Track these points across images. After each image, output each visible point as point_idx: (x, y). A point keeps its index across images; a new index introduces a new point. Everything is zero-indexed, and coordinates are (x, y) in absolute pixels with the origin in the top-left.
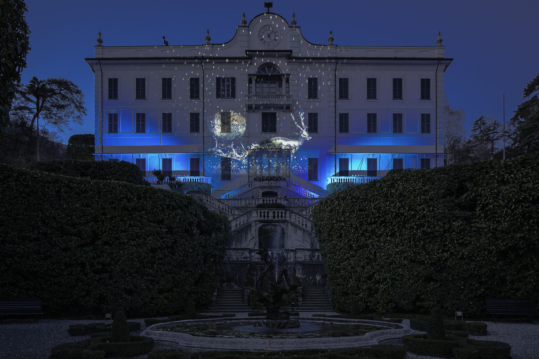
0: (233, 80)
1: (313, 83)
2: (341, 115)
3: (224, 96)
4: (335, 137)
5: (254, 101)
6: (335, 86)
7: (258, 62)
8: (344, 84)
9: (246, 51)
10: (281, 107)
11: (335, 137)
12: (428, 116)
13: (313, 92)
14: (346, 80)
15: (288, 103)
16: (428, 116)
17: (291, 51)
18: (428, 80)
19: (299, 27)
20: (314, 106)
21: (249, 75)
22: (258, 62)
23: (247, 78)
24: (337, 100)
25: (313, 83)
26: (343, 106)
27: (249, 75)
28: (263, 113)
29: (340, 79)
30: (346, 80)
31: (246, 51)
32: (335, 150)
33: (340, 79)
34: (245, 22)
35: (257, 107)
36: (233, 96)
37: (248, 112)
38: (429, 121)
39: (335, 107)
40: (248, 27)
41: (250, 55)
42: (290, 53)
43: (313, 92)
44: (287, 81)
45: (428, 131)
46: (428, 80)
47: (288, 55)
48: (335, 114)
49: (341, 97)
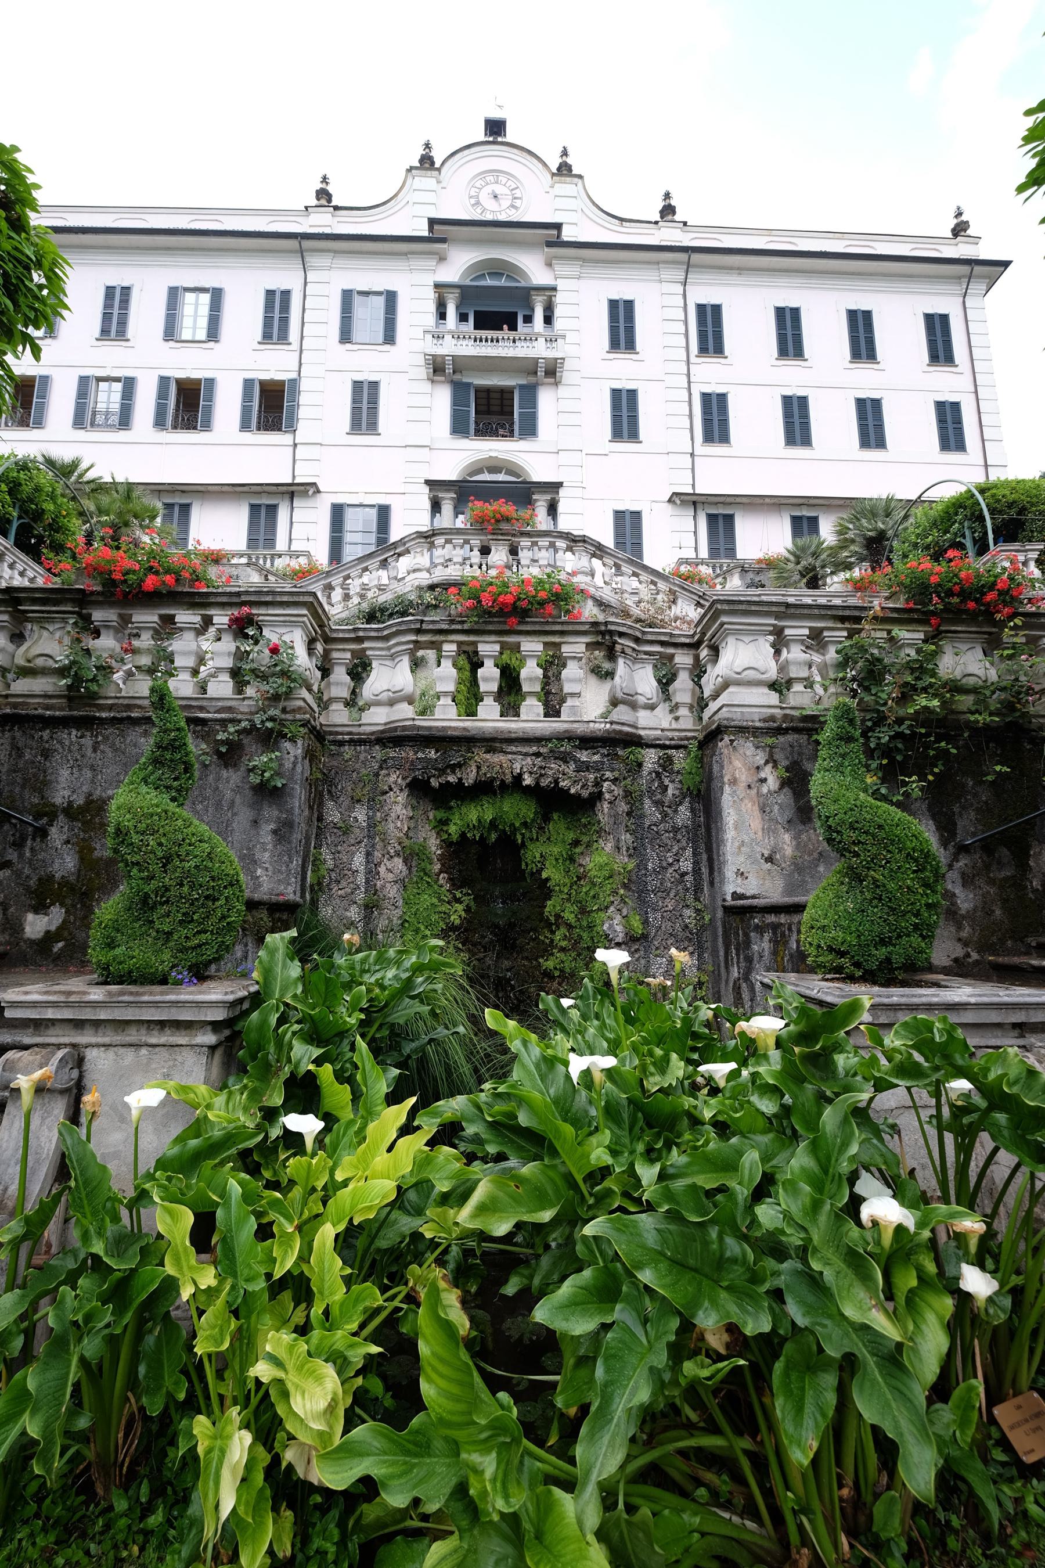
0: (391, 298)
2: (706, 397)
4: (692, 455)
5: (449, 348)
6: (686, 322)
9: (432, 222)
11: (692, 455)
12: (956, 406)
14: (717, 309)
15: (551, 354)
16: (956, 406)
17: (558, 227)
18: (944, 318)
19: (580, 177)
21: (437, 286)
23: (431, 295)
24: (693, 359)
27: (437, 286)
29: (701, 308)
30: (717, 309)
31: (432, 222)
32: (693, 485)
33: (701, 308)
34: (427, 162)
36: (390, 338)
37: (433, 382)
38: (958, 421)
39: (688, 375)
40: (439, 170)
42: (555, 232)
45: (960, 446)
46: (944, 318)
48: (690, 394)
49: (703, 350)
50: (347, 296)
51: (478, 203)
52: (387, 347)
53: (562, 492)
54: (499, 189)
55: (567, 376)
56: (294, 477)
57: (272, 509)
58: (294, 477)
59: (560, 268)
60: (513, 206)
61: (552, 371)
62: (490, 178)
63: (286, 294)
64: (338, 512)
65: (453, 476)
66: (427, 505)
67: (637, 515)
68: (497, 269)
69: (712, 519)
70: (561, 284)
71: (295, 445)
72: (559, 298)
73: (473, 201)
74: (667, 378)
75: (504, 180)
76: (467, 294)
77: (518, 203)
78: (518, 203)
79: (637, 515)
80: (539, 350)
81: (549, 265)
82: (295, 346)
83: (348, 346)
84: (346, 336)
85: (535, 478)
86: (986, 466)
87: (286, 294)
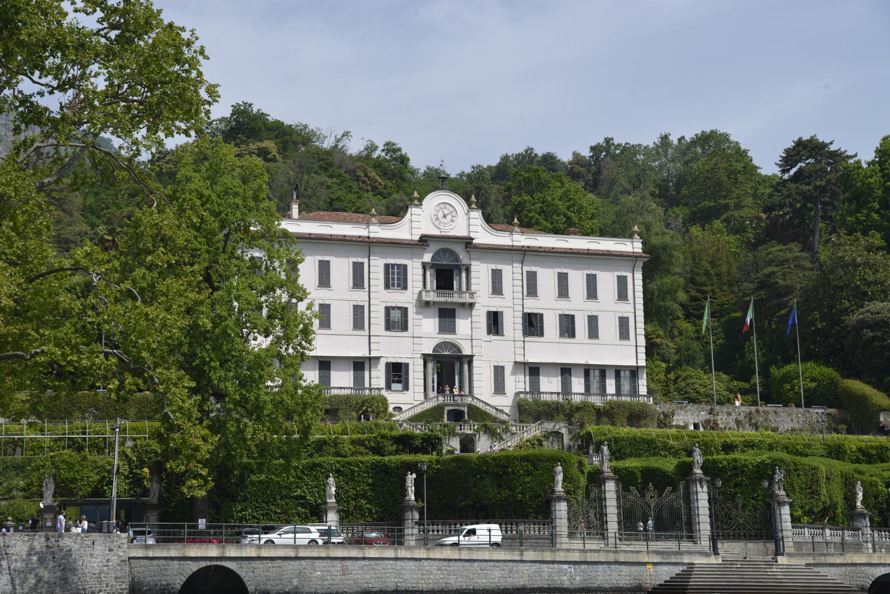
0: (405, 266)
1: (497, 276)
3: (393, 285)
5: (432, 297)
7: (435, 247)
8: (532, 278)
10: (463, 305)
12: (628, 318)
13: (497, 288)
15: (471, 301)
20: (495, 304)
22: (435, 247)
24: (525, 297)
25: (497, 276)
26: (532, 306)
28: (440, 309)
29: (527, 272)
33: (527, 272)
35: (434, 303)
41: (424, 241)
43: (497, 288)
44: (468, 270)
47: (467, 242)
50: (387, 266)
51: (438, 218)
52: (404, 291)
53: (474, 358)
54: (446, 212)
55: (477, 306)
56: (370, 350)
57: (363, 363)
58: (370, 350)
59: (473, 255)
60: (452, 221)
61: (471, 306)
62: (442, 206)
63: (363, 263)
64: (387, 364)
65: (431, 353)
66: (422, 362)
67: (503, 368)
68: (445, 251)
69: (530, 369)
70: (473, 263)
71: (370, 336)
72: (473, 268)
73: (435, 217)
74: (515, 306)
75: (448, 206)
76: (433, 266)
77: (454, 219)
78: (454, 219)
79: (503, 368)
80: (466, 299)
81: (468, 252)
82: (367, 289)
83: (389, 291)
84: (387, 286)
85: (464, 353)
86: (637, 346)
87: (363, 263)
